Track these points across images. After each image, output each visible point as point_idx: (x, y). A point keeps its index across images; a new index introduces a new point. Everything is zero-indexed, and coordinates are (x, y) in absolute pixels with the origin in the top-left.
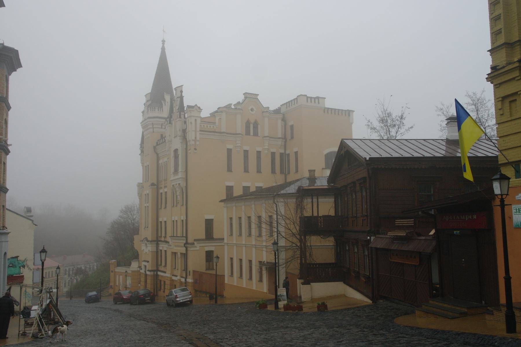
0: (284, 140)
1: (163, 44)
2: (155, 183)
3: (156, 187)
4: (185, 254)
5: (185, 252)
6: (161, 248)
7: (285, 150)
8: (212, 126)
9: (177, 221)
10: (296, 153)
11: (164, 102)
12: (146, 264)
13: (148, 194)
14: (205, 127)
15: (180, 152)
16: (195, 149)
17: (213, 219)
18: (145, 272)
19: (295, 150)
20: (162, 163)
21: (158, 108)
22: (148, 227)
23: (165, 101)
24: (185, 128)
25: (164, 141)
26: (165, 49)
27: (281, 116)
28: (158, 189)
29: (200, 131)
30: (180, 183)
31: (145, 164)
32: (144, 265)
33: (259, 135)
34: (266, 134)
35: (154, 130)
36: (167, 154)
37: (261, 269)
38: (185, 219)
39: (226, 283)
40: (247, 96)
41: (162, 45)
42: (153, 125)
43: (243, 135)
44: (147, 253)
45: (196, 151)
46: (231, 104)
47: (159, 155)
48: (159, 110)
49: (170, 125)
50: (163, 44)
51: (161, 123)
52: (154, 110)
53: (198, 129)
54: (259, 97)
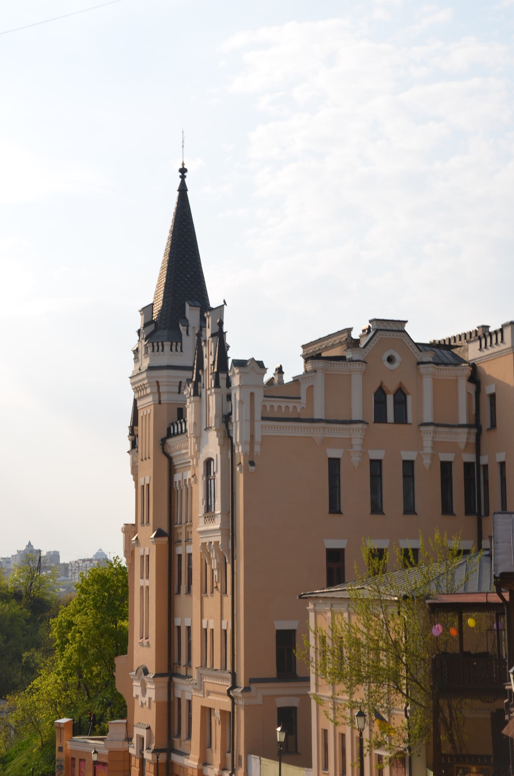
0: (474, 431)
1: (183, 177)
2: (165, 529)
3: (165, 539)
6: (178, 694)
7: (478, 454)
8: (291, 406)
10: (502, 464)
11: (186, 328)
13: (148, 556)
14: (276, 409)
16: (252, 463)
19: (501, 457)
20: (180, 482)
21: (170, 343)
23: (188, 327)
24: (230, 411)
26: (187, 190)
27: (467, 371)
28: (172, 543)
29: (263, 419)
30: (218, 542)
31: (141, 482)
32: (137, 735)
33: (410, 419)
34: (428, 418)
35: (162, 399)
40: (378, 328)
41: (180, 179)
43: (367, 424)
45: (252, 468)
48: (174, 348)
49: (197, 398)
50: (183, 177)
51: (179, 381)
53: (258, 416)
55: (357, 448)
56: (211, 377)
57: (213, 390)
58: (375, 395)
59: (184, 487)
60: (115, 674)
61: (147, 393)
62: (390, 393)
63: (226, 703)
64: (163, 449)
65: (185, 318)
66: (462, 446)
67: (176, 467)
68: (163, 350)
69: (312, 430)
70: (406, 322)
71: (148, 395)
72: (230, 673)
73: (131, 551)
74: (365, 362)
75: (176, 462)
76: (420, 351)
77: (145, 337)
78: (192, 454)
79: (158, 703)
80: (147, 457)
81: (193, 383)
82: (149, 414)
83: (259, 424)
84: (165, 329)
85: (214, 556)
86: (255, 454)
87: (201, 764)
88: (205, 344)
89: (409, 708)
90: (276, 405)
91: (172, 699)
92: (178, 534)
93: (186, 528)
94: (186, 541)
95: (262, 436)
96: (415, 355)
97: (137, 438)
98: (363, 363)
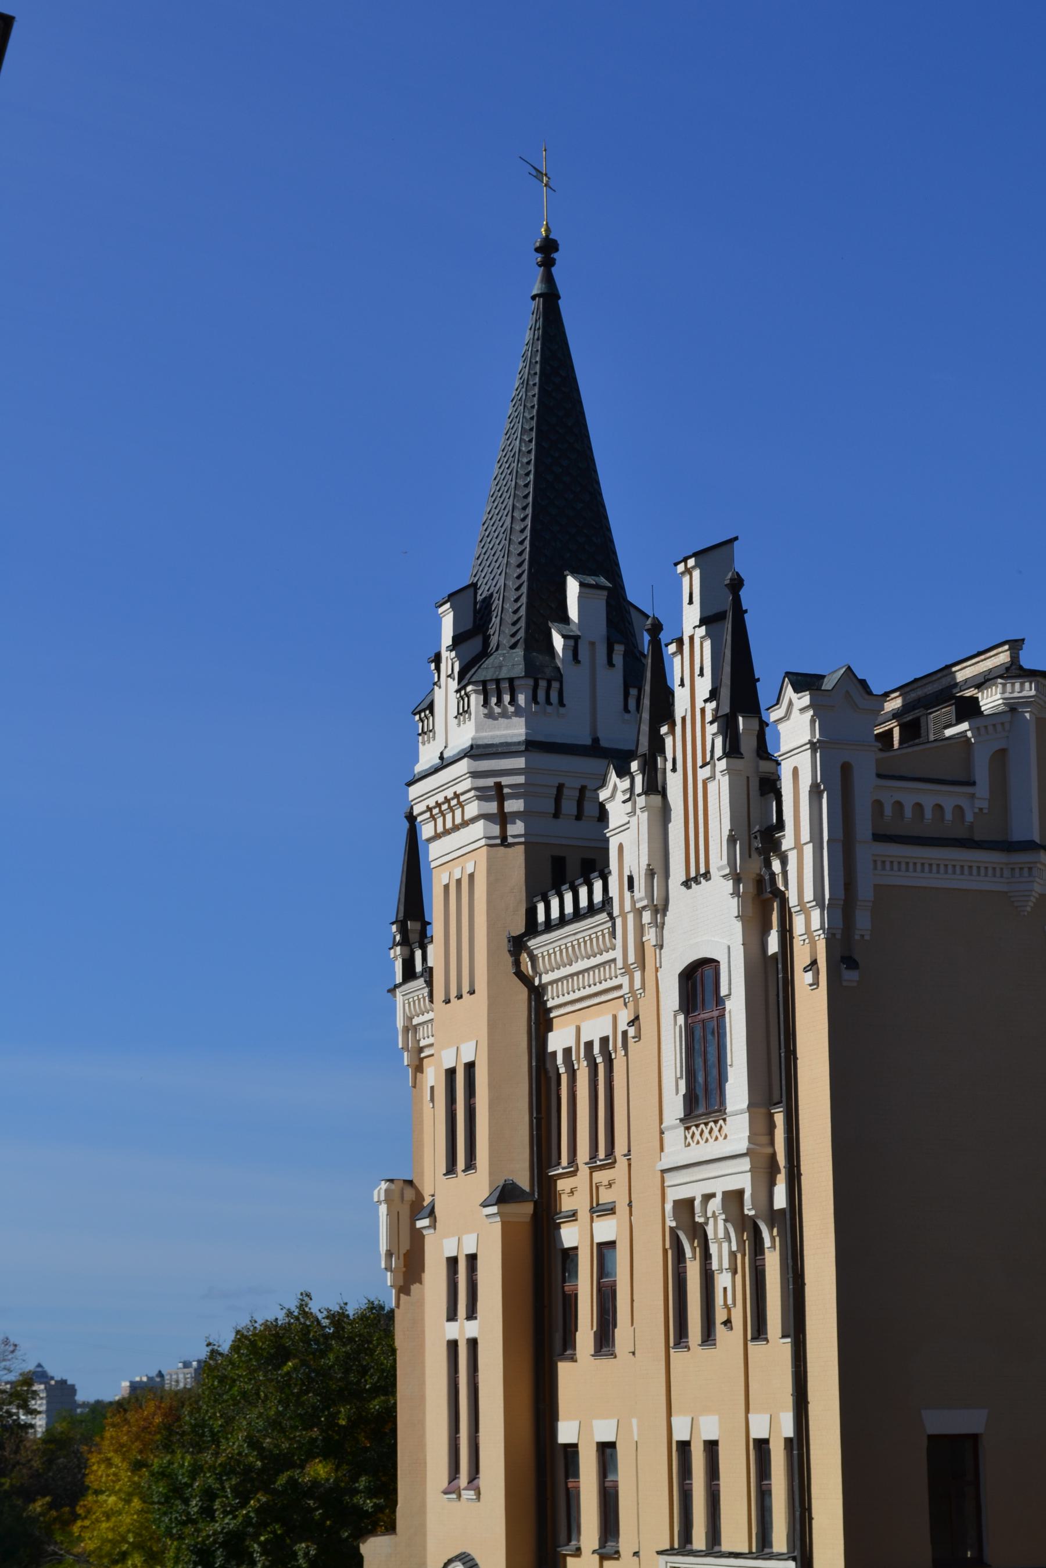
1: (548, 263)
2: (524, 1182)
3: (528, 1208)
9: (712, 1447)
13: (472, 1259)
14: (908, 813)
17: (974, 1439)
20: (567, 1051)
21: (530, 682)
25: (584, 903)
26: (559, 298)
29: (879, 837)
30: (740, 1193)
36: (620, 987)
38: (788, 1429)
42: (501, 799)
45: (850, 976)
49: (657, 799)
50: (548, 263)
52: (507, 698)
53: (864, 828)
56: (712, 729)
57: (722, 765)
61: (466, 817)
64: (517, 963)
65: (565, 619)
67: (552, 1015)
68: (513, 701)
71: (465, 824)
72: (794, 1559)
73: (403, 1251)
78: (631, 959)
80: (466, 988)
82: (471, 876)
83: (866, 852)
84: (513, 646)
85: (721, 1234)
86: (857, 937)
88: (680, 650)
90: (908, 802)
93: (591, 1173)
94: (592, 1210)
95: (877, 887)
97: (418, 954)
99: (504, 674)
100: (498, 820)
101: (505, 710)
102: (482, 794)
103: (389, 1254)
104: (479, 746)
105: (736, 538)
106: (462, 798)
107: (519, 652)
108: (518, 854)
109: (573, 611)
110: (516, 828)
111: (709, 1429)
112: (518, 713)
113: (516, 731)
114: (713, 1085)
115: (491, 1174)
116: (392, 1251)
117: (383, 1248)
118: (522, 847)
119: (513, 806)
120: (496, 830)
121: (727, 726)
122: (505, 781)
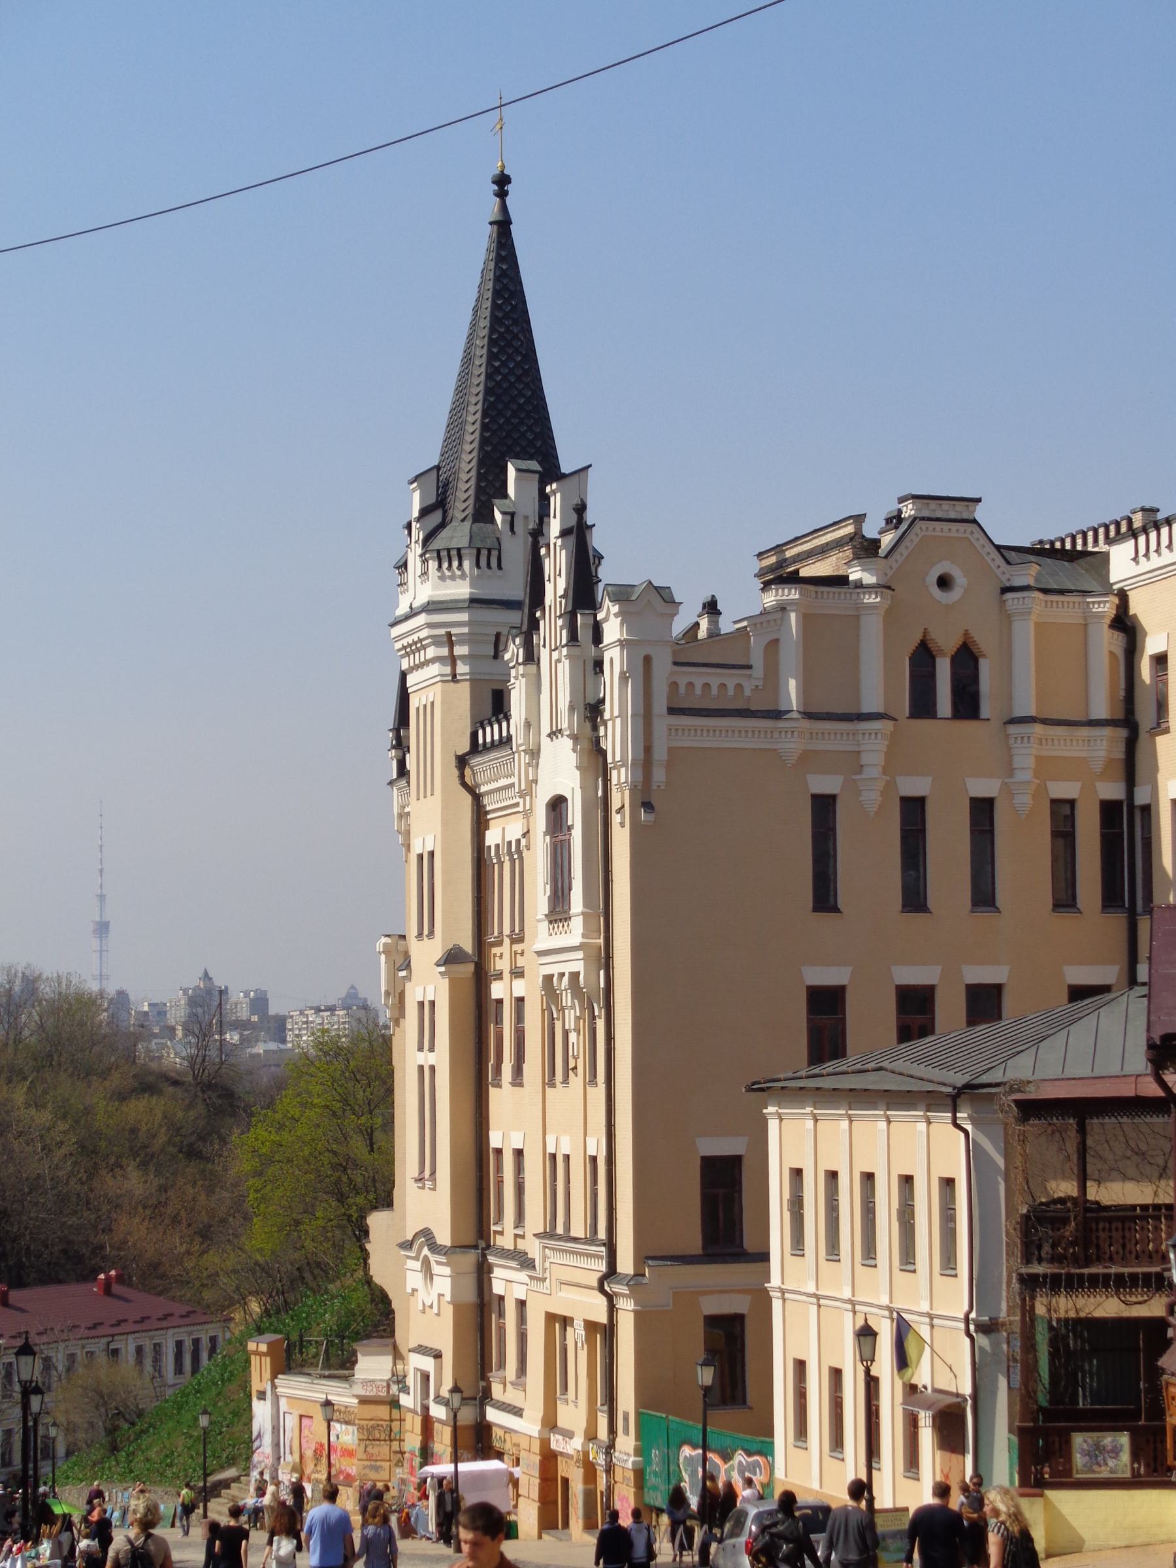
0: (1123, 733)
1: (502, 194)
3: (471, 968)
4: (605, 1325)
5: (603, 1319)
6: (498, 1288)
8: (731, 684)
12: (428, 1364)
13: (432, 1004)
14: (698, 691)
15: (575, 815)
16: (648, 806)
18: (426, 1409)
20: (497, 846)
21: (475, 551)
22: (433, 1173)
24: (602, 695)
27: (1106, 607)
28: (482, 977)
29: (672, 711)
30: (578, 973)
32: (416, 1369)
33: (985, 710)
36: (517, 805)
37: (912, 1423)
38: (604, 1154)
39: (780, 1480)
42: (451, 645)
44: (431, 1307)
46: (859, 519)
47: (486, 800)
49: (532, 668)
50: (502, 194)
52: (455, 564)
53: (660, 705)
54: (980, 513)
55: (873, 772)
56: (560, 622)
57: (565, 651)
58: (910, 658)
59: (507, 858)
60: (368, 1246)
62: (942, 653)
63: (596, 1308)
64: (462, 777)
65: (505, 496)
66: (1098, 767)
67: (489, 817)
68: (460, 565)
69: (776, 735)
70: (979, 500)
71: (427, 663)
72: (604, 1245)
74: (889, 588)
75: (490, 804)
76: (1008, 563)
77: (421, 538)
78: (523, 787)
79: (458, 1307)
81: (523, 636)
84: (463, 520)
85: (569, 1004)
86: (654, 788)
87: (547, 1429)
89: (973, 1315)
91: (486, 1298)
92: (495, 956)
94: (511, 973)
95: (671, 750)
96: (998, 572)
98: (884, 590)
99: (454, 544)
100: (449, 661)
101: (454, 572)
102: (436, 641)
103: (387, 994)
104: (434, 603)
105: (591, 466)
106: (424, 643)
107: (468, 524)
108: (464, 690)
109: (511, 490)
110: (462, 668)
111: (565, 1149)
112: (463, 577)
113: (462, 591)
114: (566, 891)
115: (443, 941)
116: (391, 991)
117: (383, 990)
118: (467, 684)
119: (460, 650)
120: (448, 670)
121: (570, 618)
122: (454, 631)
